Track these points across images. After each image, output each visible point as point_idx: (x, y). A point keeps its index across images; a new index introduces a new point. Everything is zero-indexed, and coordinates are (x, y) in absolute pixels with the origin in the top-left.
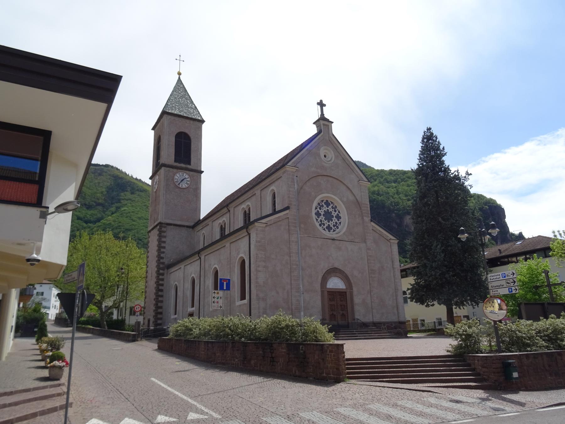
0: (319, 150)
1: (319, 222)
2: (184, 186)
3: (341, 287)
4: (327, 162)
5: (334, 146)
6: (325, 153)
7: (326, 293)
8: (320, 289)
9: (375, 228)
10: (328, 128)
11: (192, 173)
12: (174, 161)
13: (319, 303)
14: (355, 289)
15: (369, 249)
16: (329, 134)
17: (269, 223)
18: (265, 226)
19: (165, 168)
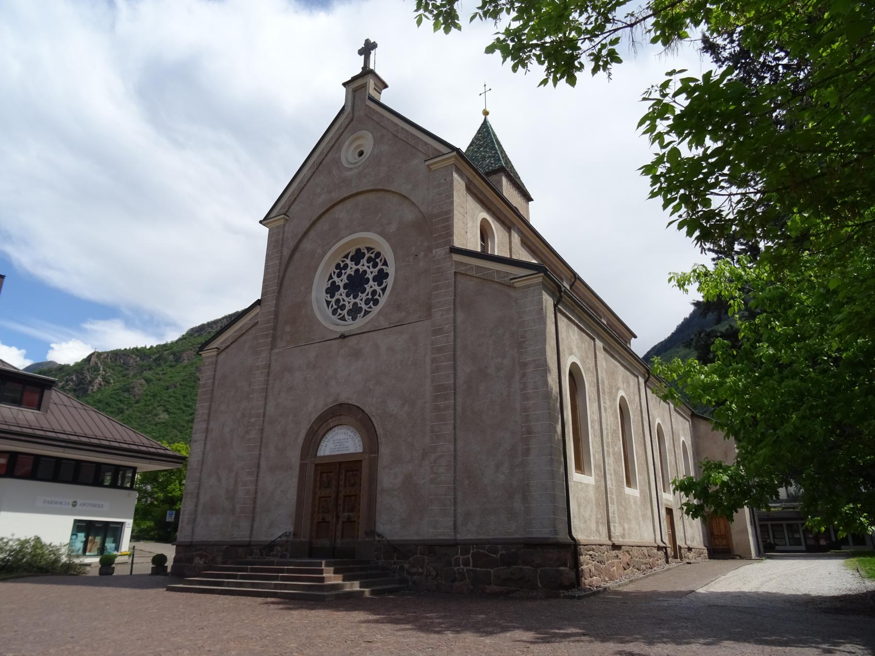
3: (352, 450)
7: (311, 470)
8: (299, 460)
9: (466, 265)
13: (292, 494)
14: (385, 451)
15: (437, 331)
17: (224, 346)
18: (215, 353)
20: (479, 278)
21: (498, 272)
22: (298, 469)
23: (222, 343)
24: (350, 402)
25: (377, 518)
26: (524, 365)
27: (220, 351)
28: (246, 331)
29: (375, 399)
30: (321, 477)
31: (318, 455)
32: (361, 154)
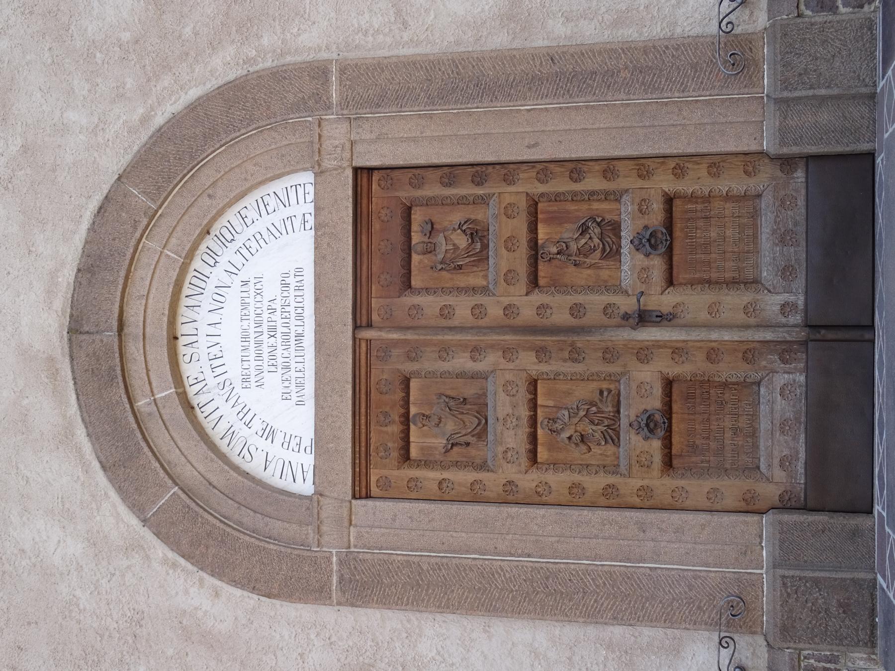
24: (68, 275)
25: (656, 31)
29: (72, 116)
30: (426, 463)
31: (306, 487)
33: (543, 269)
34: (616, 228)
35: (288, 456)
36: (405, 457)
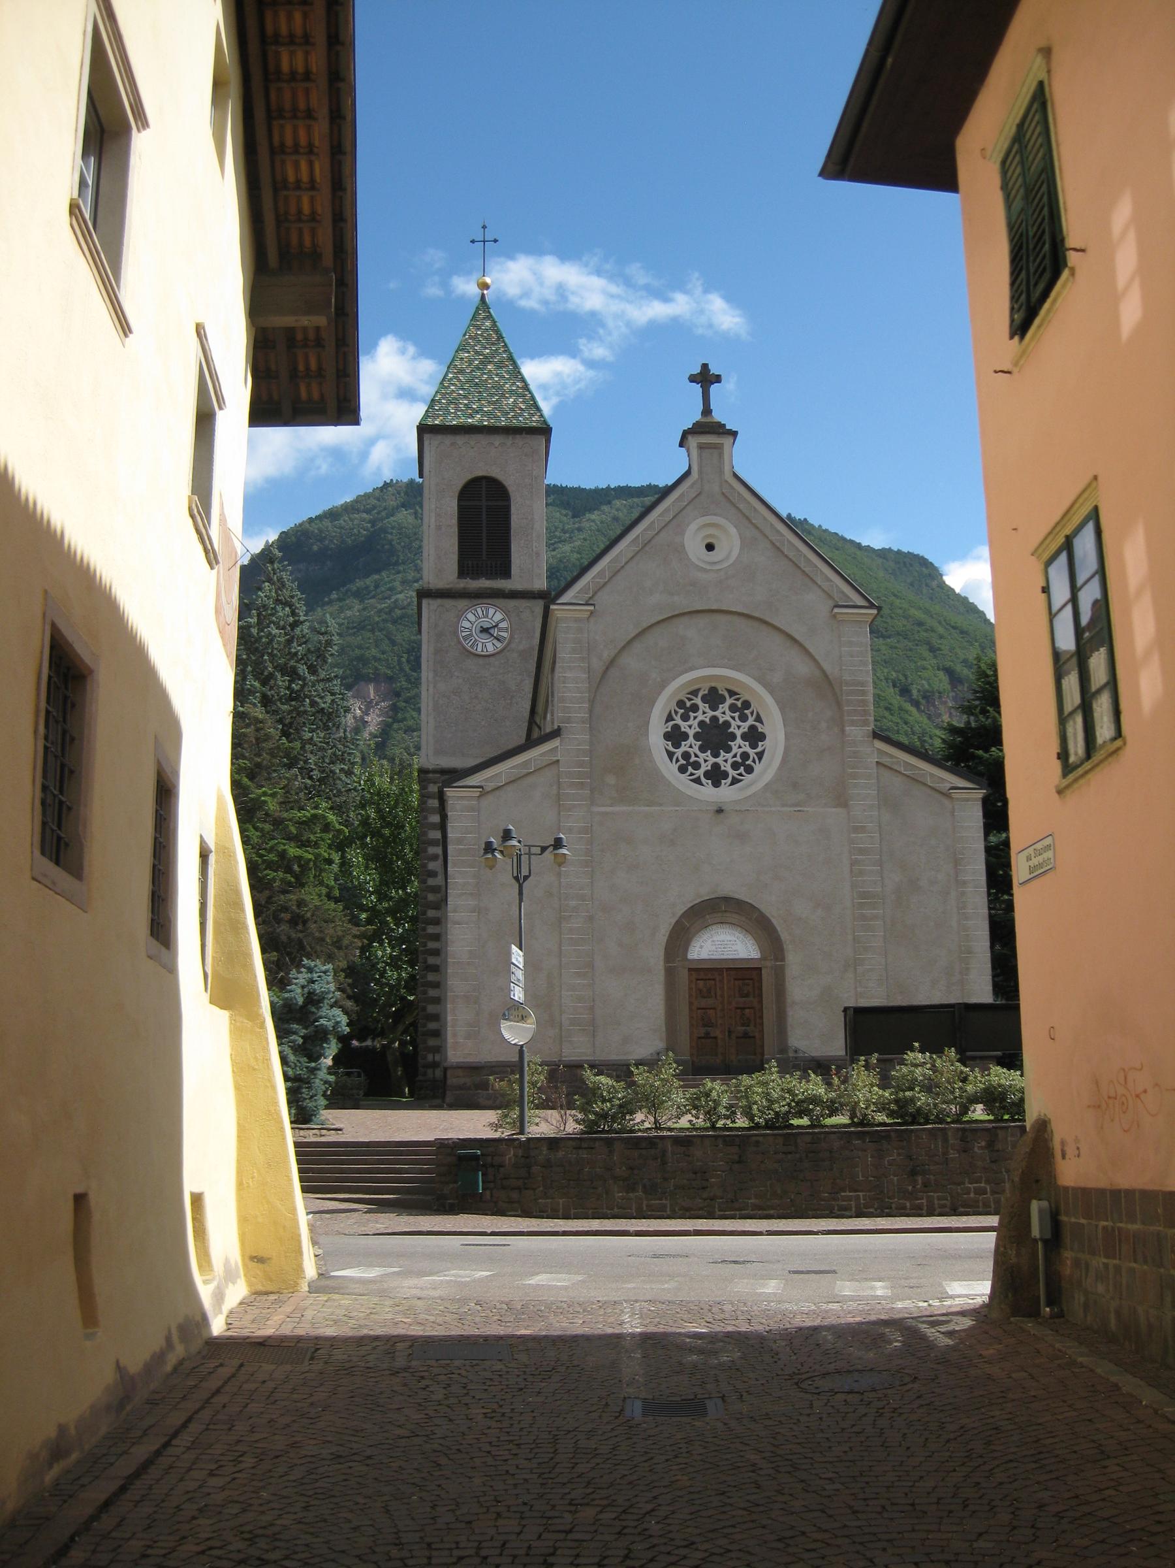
0: (682, 533)
1: (677, 760)
2: (491, 649)
4: (708, 567)
5: (738, 508)
6: (710, 536)
7: (683, 976)
8: (662, 963)
9: (891, 756)
10: (721, 455)
11: (512, 603)
12: (457, 575)
14: (794, 960)
16: (721, 472)
17: (490, 786)
18: (478, 794)
19: (431, 601)
20: (908, 776)
21: (932, 775)
22: (662, 972)
23: (486, 780)
24: (736, 896)
26: (964, 883)
27: (483, 792)
28: (535, 771)
32: (710, 547)
33: (739, 1011)
34: (748, 1026)
35: (696, 953)
36: (698, 980)
